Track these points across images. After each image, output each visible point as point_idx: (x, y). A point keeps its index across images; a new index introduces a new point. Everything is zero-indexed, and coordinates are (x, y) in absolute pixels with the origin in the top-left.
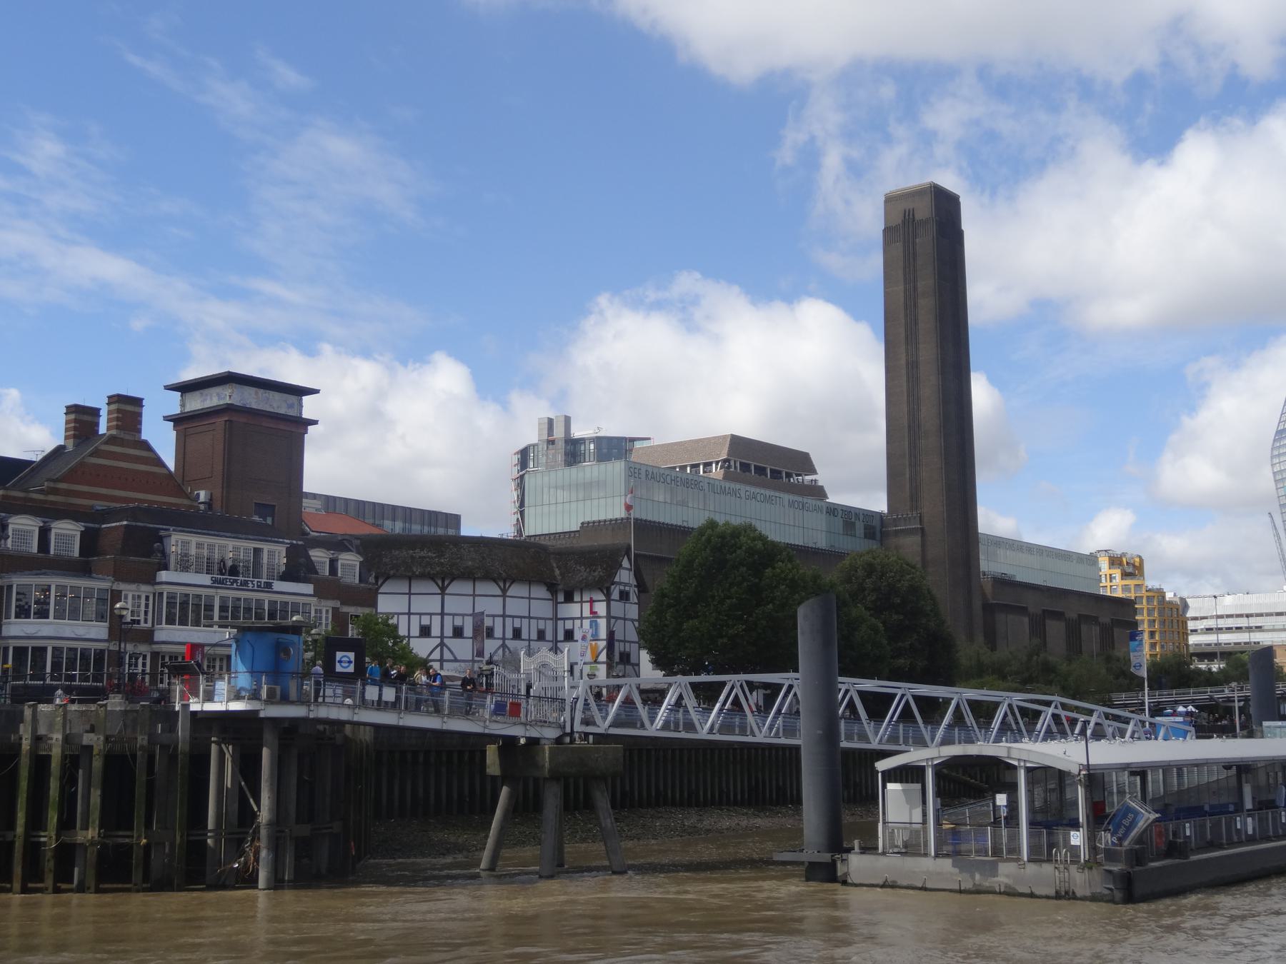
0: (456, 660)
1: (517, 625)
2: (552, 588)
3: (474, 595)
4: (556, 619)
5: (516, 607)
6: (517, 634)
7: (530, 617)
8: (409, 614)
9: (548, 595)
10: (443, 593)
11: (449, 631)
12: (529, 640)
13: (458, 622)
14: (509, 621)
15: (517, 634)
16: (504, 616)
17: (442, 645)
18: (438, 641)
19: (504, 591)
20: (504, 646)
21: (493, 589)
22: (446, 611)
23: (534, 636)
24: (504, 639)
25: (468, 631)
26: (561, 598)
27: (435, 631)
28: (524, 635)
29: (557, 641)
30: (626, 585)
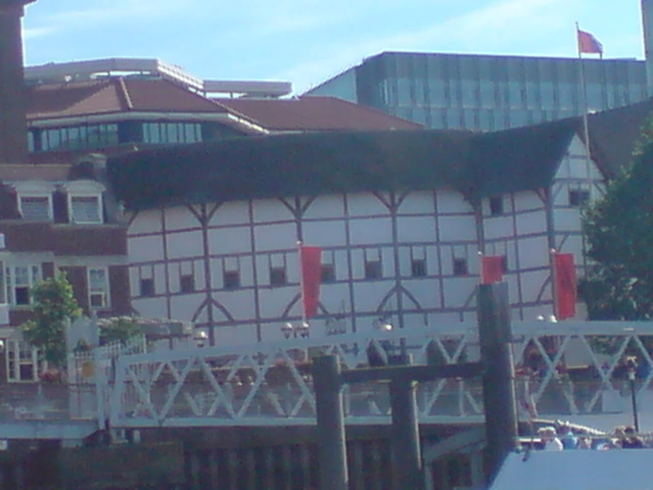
1: (417, 256)
2: (471, 195)
3: (346, 219)
4: (480, 242)
6: (419, 269)
7: (438, 243)
9: (466, 207)
10: (298, 221)
14: (403, 252)
15: (419, 269)
16: (395, 245)
19: (393, 207)
20: (398, 289)
23: (448, 268)
24: (398, 278)
25: (294, 273)
26: (486, 208)
28: (431, 269)
30: (580, 181)
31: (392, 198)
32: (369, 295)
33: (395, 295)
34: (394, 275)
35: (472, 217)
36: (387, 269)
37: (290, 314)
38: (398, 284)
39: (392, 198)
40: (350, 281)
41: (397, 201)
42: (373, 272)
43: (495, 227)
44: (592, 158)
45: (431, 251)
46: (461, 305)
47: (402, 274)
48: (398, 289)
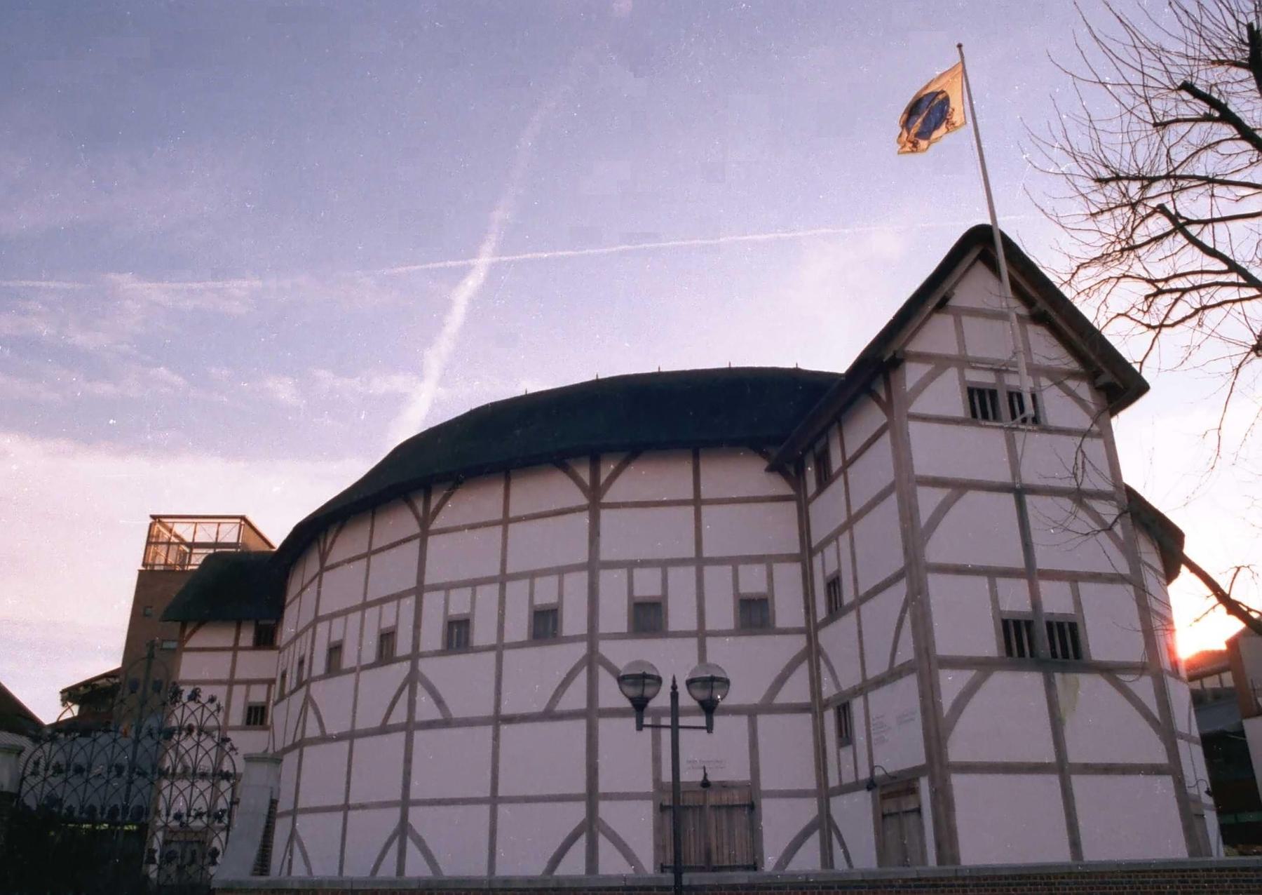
0: (447, 723)
5: (624, 533)
7: (700, 561)
8: (365, 605)
9: (779, 486)
11: (433, 637)
12: (701, 634)
13: (459, 604)
17: (413, 679)
18: (405, 667)
19: (595, 493)
21: (558, 490)
22: (428, 581)
24: (592, 636)
27: (403, 645)
28: (680, 615)
29: (818, 627)
31: (595, 475)
32: (536, 674)
33: (585, 670)
34: (583, 630)
35: (793, 506)
36: (573, 621)
37: (392, 721)
38: (593, 649)
39: (595, 475)
40: (499, 648)
41: (603, 477)
42: (545, 624)
43: (828, 511)
44: (1038, 318)
45: (682, 579)
46: (756, 699)
47: (603, 628)
48: (592, 661)
